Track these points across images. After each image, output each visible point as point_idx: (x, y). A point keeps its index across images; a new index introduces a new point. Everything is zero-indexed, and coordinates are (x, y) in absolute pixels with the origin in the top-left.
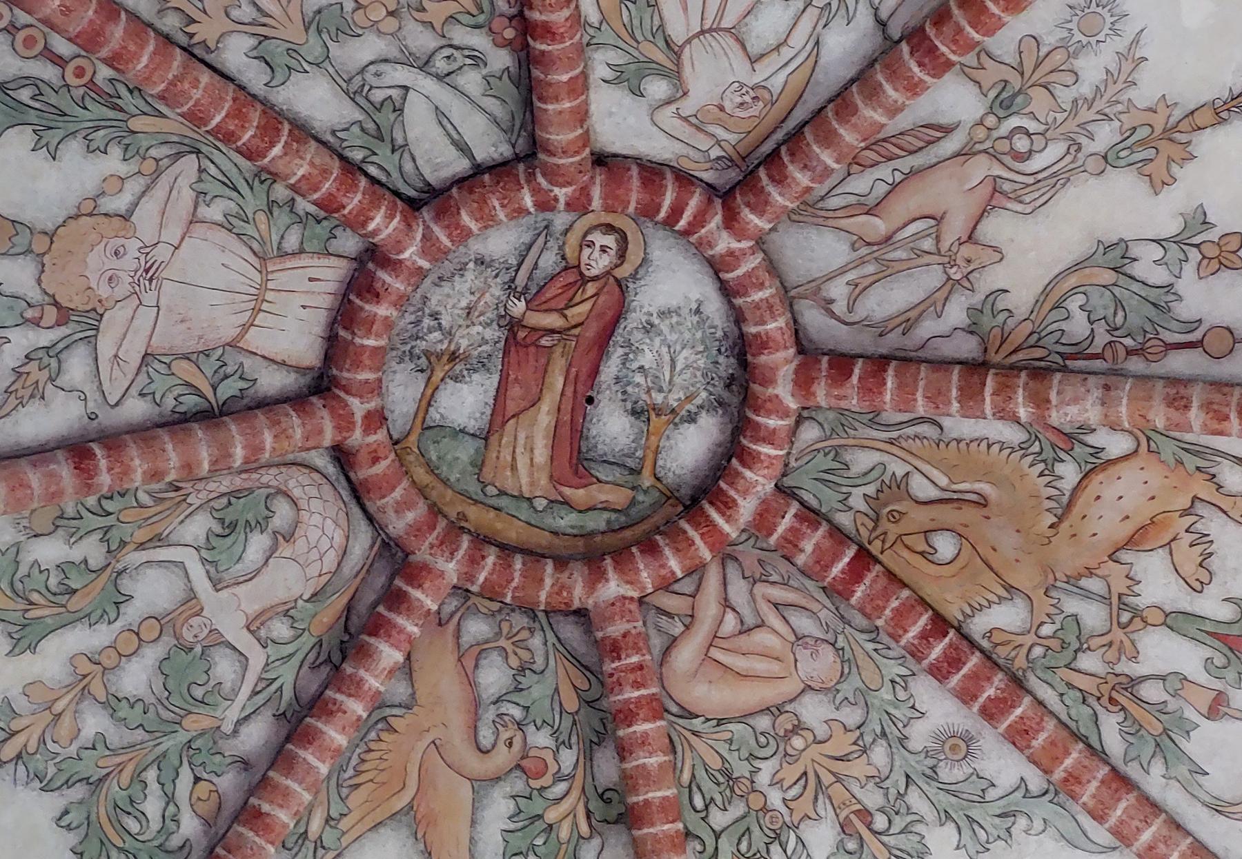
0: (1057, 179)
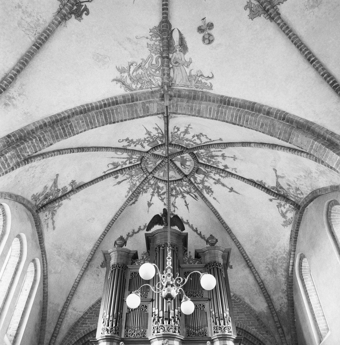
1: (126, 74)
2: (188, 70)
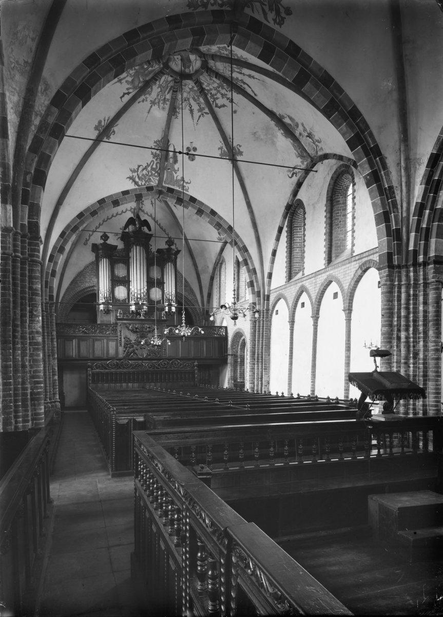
0: (158, 95)
1: (136, 174)
2: (175, 175)
